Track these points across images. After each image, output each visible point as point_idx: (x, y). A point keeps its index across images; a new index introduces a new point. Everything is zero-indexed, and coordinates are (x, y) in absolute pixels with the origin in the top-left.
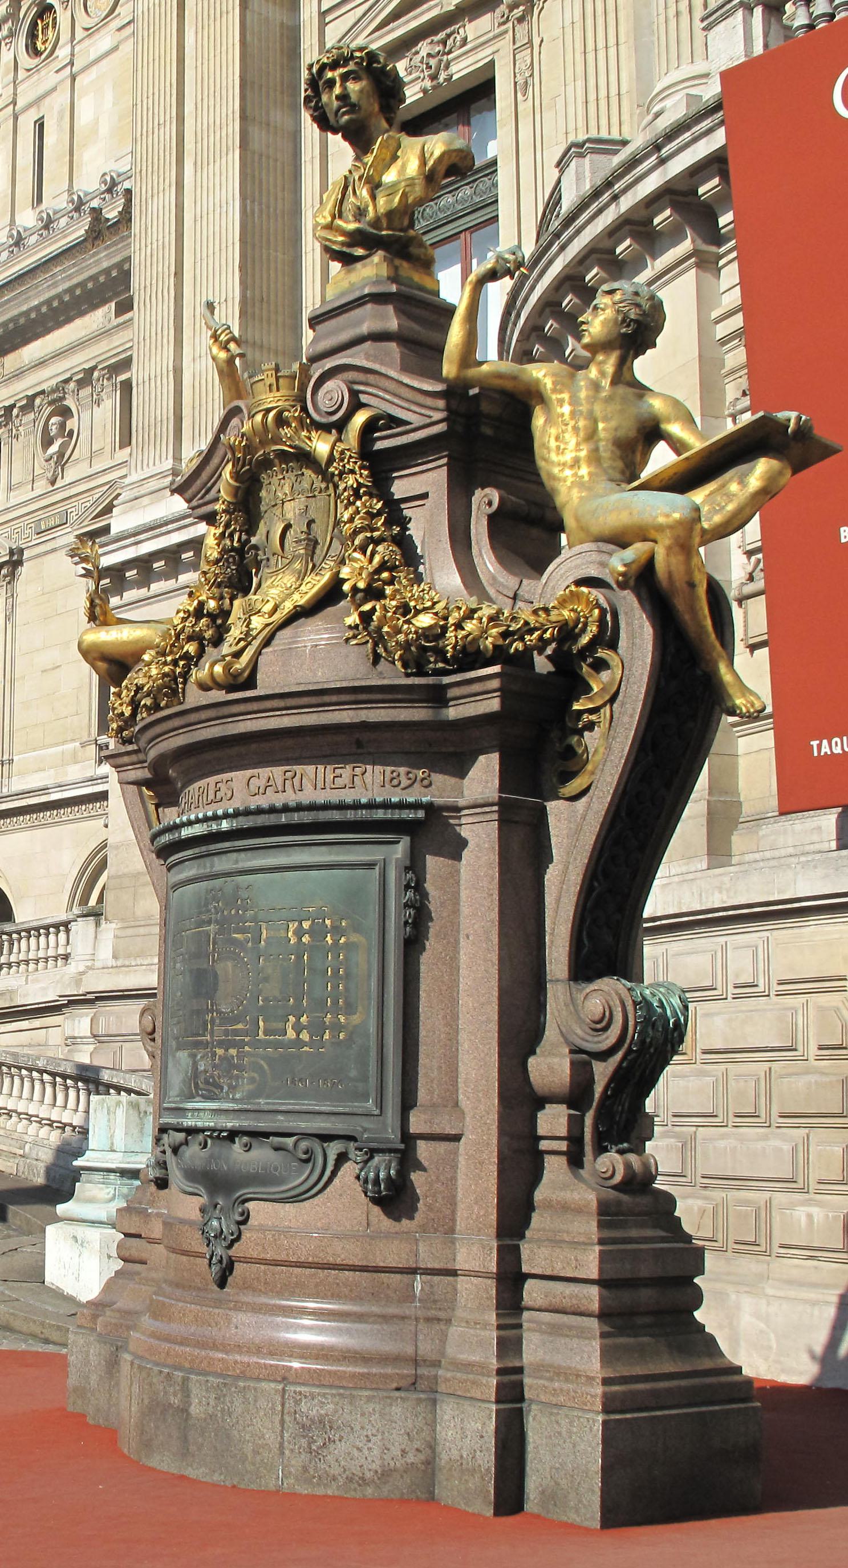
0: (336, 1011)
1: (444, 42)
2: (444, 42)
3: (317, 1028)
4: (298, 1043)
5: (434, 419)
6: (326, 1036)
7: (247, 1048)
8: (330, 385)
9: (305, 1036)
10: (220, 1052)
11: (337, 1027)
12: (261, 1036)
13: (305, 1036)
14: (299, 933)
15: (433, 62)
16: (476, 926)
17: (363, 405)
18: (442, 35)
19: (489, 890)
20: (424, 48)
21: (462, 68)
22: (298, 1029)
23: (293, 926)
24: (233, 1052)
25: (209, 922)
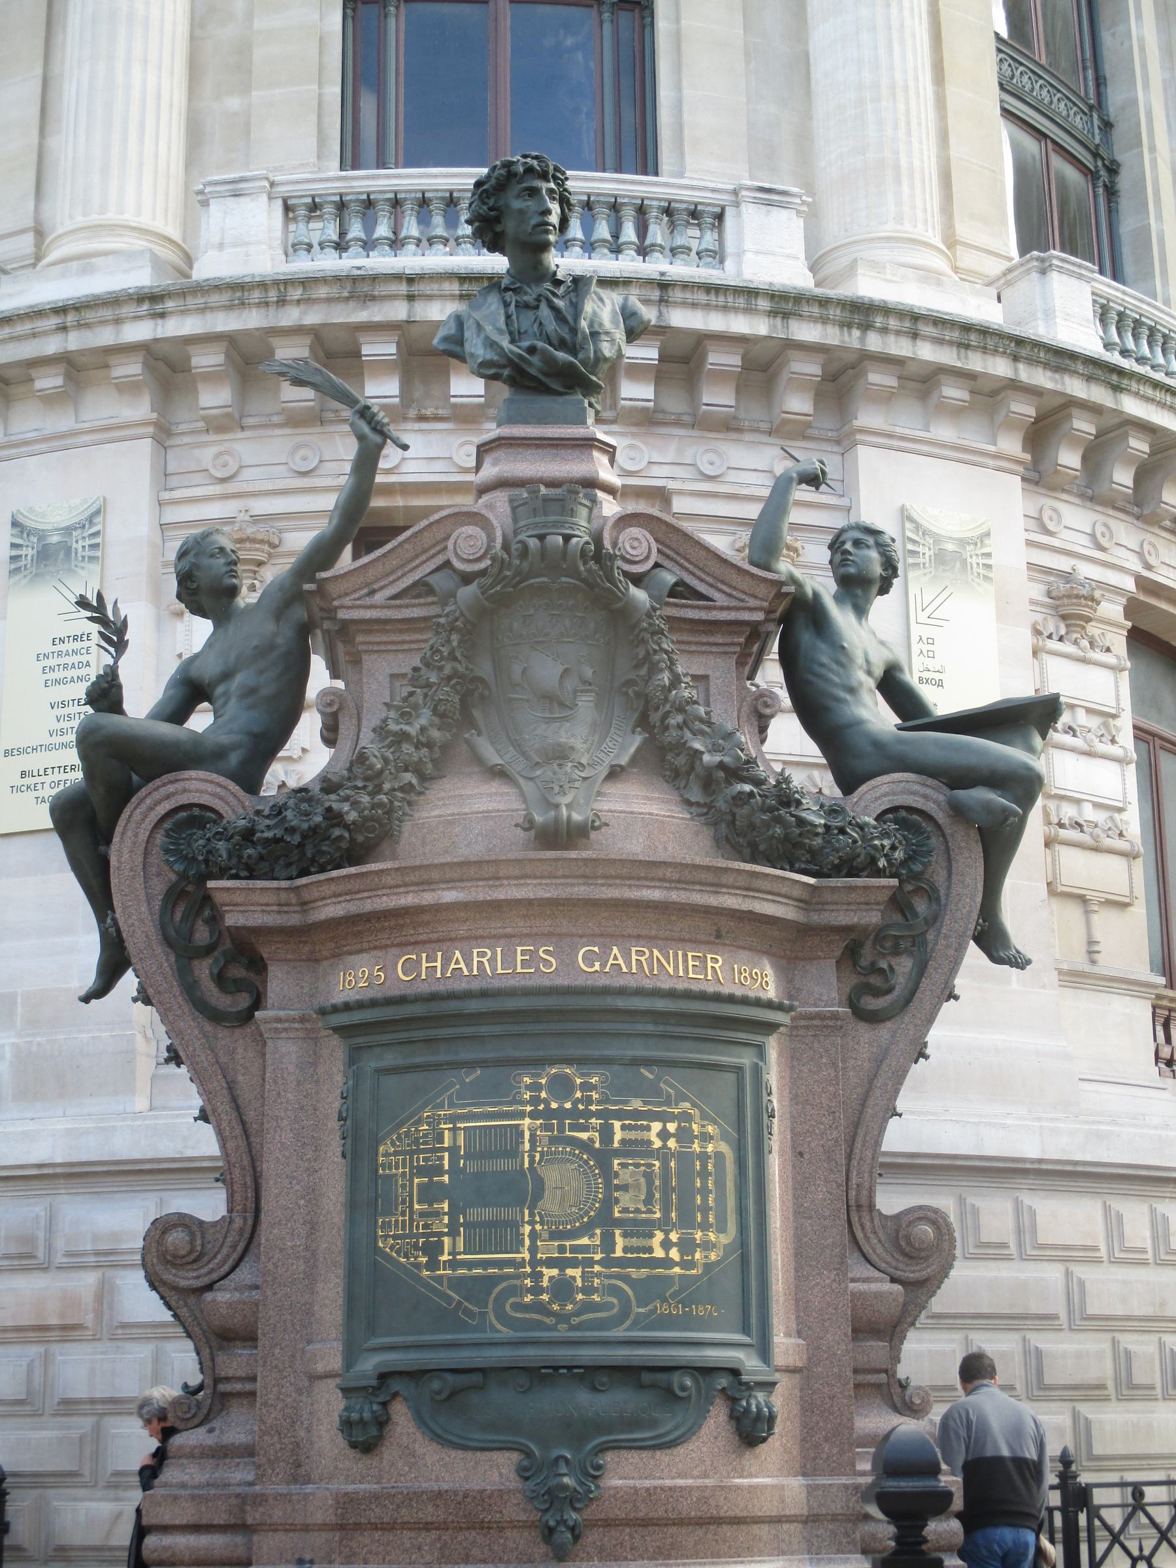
0: (705, 1226)
3: (687, 1246)
4: (667, 1263)
6: (697, 1256)
7: (597, 1268)
9: (674, 1254)
10: (550, 1273)
11: (707, 1246)
12: (619, 1253)
13: (674, 1254)
14: (664, 1135)
16: (813, 1145)
19: (830, 1107)
22: (666, 1244)
23: (656, 1126)
24: (575, 1272)
25: (522, 1115)
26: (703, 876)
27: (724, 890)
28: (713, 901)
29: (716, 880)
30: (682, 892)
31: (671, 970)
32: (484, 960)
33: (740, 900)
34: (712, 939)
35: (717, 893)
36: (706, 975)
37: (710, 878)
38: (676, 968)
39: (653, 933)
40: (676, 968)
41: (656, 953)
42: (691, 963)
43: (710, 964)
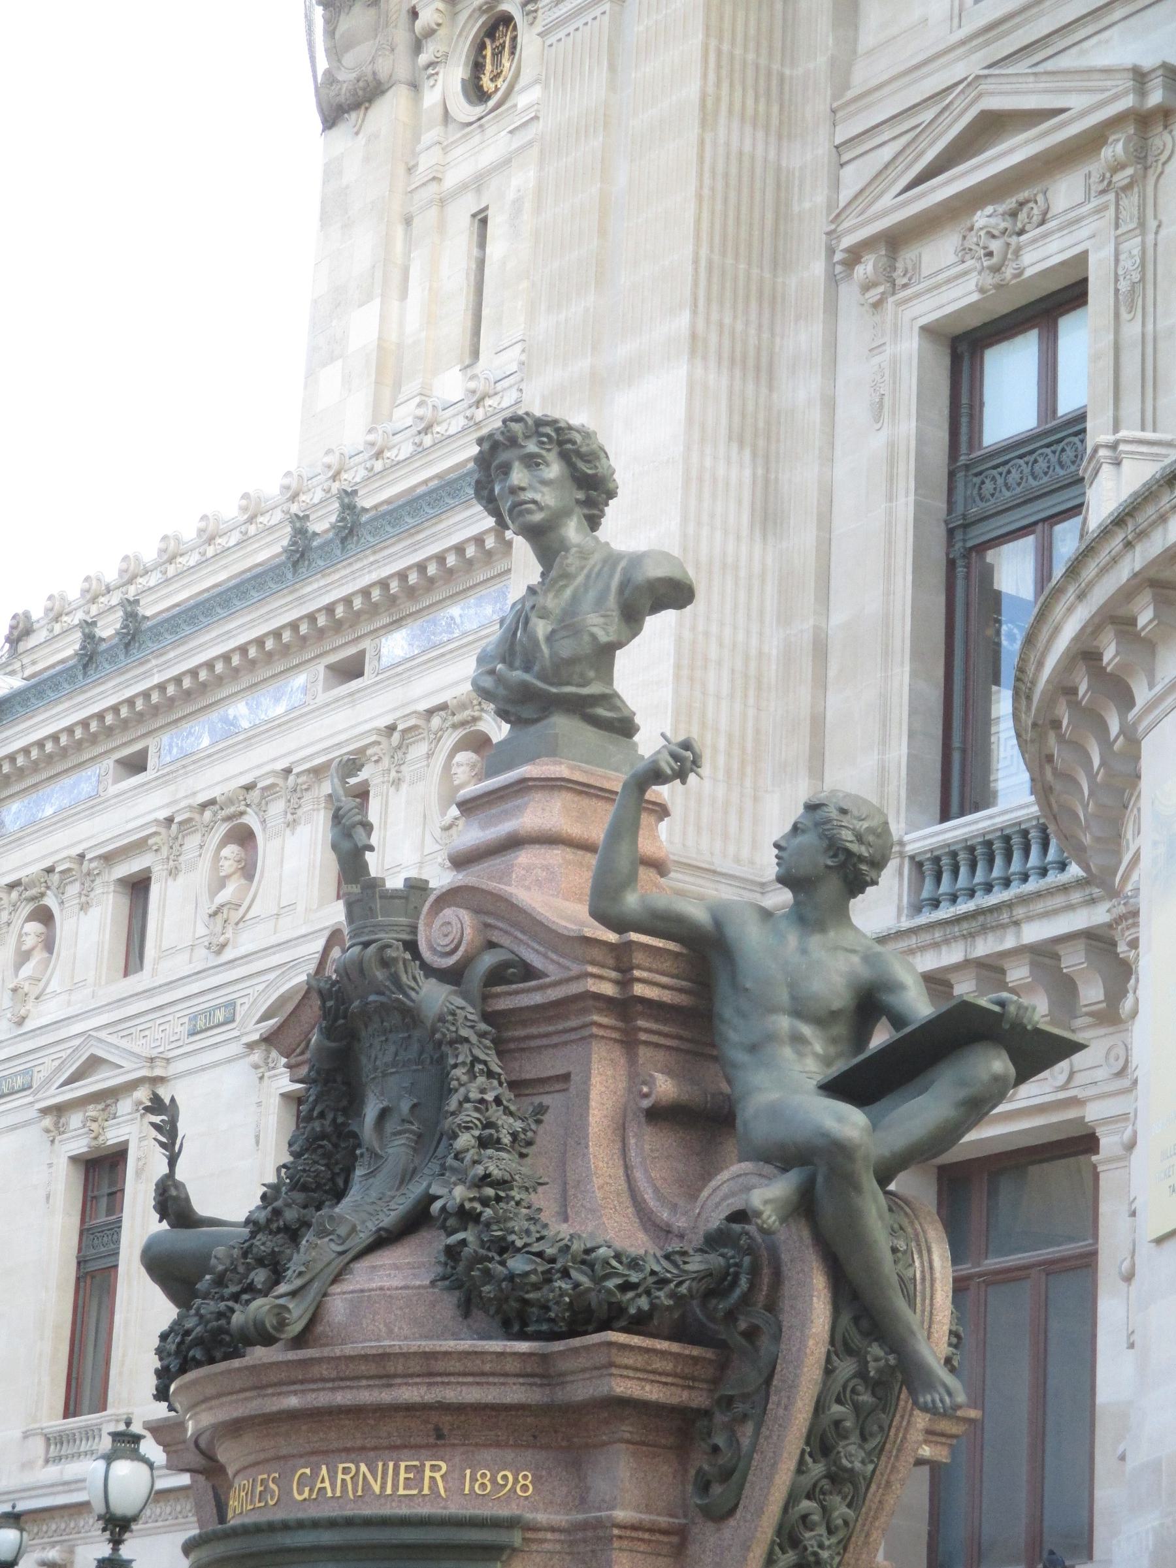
1: (1014, 214)
2: (1014, 214)
5: (572, 973)
8: (448, 913)
15: (995, 246)
17: (491, 945)
18: (1010, 203)
20: (982, 218)
21: (1041, 256)
26: (363, 1368)
27: (399, 1381)
28: (385, 1397)
29: (382, 1372)
30: (348, 1391)
31: (377, 1489)
32: (437, 1475)
33: (423, 1389)
34: (432, 1440)
35: (391, 1386)
36: (421, 1490)
37: (373, 1369)
38: (383, 1487)
39: (359, 1443)
40: (383, 1487)
41: (363, 1468)
42: (403, 1475)
43: (428, 1473)
